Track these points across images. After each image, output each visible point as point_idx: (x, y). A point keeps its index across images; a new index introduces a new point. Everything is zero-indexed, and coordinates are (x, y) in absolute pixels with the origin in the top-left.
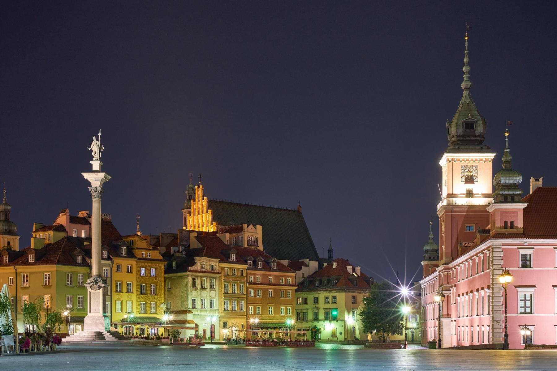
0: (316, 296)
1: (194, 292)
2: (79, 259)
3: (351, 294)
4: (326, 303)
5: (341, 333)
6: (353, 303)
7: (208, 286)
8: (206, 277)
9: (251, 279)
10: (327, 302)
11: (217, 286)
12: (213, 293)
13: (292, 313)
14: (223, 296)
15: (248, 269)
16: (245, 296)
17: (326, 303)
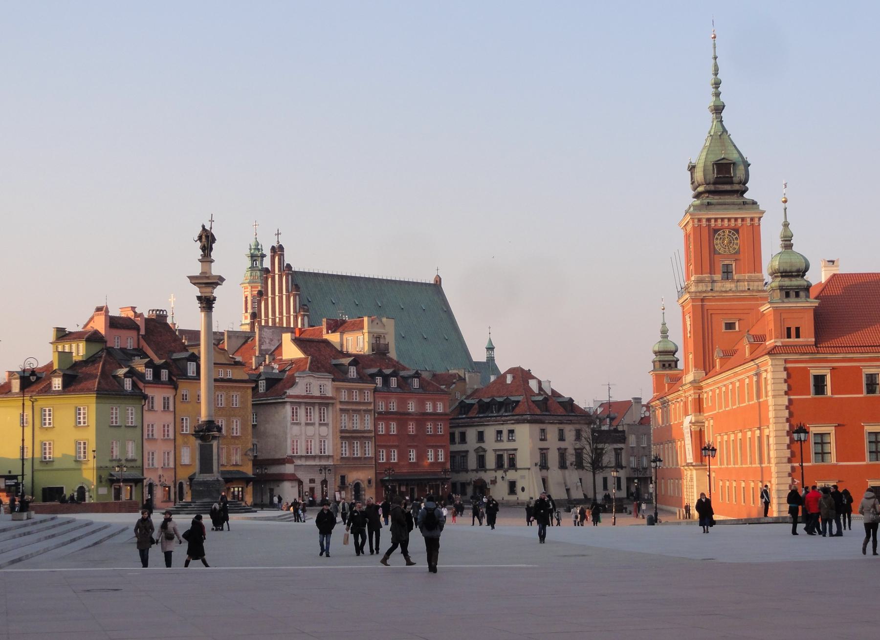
0: (481, 429)
1: (296, 429)
2: (128, 384)
3: (537, 427)
4: (497, 441)
5: (523, 489)
6: (541, 440)
7: (315, 416)
8: (313, 404)
9: (382, 407)
10: (498, 439)
11: (330, 419)
12: (324, 430)
13: (446, 458)
14: (339, 434)
15: (376, 390)
16: (373, 434)
17: (497, 441)
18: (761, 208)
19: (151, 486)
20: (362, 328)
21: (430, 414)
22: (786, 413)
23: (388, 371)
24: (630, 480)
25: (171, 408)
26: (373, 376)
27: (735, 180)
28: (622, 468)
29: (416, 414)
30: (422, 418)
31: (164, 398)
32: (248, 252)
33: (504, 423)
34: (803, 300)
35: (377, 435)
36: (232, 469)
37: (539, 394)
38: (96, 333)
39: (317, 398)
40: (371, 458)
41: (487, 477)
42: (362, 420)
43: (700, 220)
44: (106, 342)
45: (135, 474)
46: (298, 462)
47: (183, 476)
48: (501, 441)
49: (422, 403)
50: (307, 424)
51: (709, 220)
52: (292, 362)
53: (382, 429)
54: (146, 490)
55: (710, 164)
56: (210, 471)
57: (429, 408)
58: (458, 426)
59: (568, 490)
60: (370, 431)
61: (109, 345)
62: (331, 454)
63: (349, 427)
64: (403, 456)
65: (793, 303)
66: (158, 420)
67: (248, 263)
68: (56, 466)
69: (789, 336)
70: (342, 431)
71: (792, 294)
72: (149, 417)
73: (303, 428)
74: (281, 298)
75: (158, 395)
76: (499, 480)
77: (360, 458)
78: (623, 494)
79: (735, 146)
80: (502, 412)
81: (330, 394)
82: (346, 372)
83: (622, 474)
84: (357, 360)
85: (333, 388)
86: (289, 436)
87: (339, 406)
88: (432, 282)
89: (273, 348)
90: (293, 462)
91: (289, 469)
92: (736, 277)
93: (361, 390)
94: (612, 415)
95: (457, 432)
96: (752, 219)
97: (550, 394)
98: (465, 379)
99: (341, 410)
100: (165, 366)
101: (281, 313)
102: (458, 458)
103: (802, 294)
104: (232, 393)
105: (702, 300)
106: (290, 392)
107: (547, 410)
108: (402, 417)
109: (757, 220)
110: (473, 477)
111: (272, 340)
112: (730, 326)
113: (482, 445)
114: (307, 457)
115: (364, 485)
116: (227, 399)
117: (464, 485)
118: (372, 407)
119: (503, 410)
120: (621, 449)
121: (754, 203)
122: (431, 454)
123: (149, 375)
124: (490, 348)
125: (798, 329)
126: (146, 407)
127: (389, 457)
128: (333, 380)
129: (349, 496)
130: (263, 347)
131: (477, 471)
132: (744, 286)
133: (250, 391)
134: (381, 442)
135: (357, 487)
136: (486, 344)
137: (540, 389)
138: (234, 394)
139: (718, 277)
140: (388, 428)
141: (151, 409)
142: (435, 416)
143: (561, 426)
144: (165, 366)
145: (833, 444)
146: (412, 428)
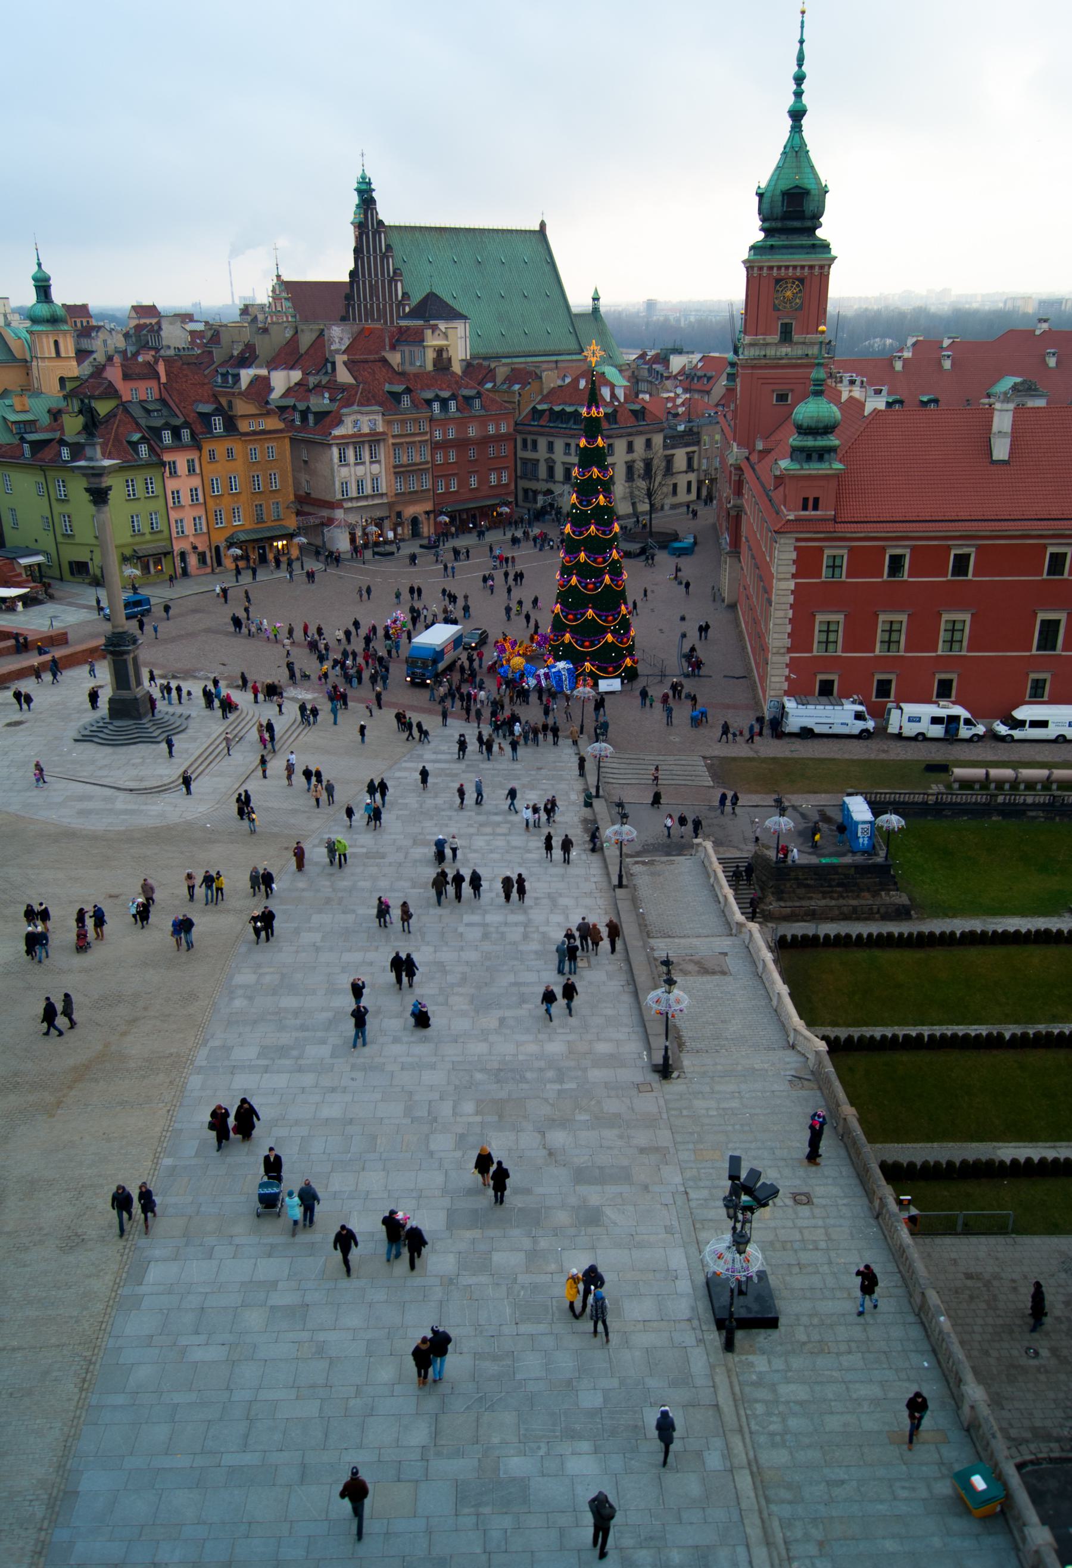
0: (551, 439)
1: (344, 471)
2: (143, 449)
4: (565, 454)
9: (438, 435)
12: (375, 468)
13: (510, 478)
14: (392, 470)
15: (431, 420)
16: (430, 465)
17: (565, 454)
18: (833, 253)
19: (183, 555)
20: (423, 341)
21: (492, 436)
22: (791, 599)
23: (445, 394)
24: (700, 483)
25: (198, 471)
26: (429, 402)
27: (808, 213)
28: (693, 471)
30: (485, 441)
31: (188, 461)
32: (356, 186)
33: (572, 436)
34: (825, 465)
35: (434, 466)
36: (273, 524)
37: (607, 405)
38: (111, 384)
39: (366, 435)
40: (428, 490)
41: (558, 489)
43: (761, 268)
44: (121, 397)
45: (161, 545)
46: (349, 505)
47: (219, 539)
48: (569, 454)
49: (484, 425)
50: (356, 464)
51: (771, 268)
52: (344, 388)
53: (439, 458)
54: (178, 560)
55: (778, 192)
56: (129, 689)
57: (491, 430)
58: (530, 433)
59: (634, 504)
60: (427, 463)
61: (124, 399)
63: (404, 460)
64: (463, 483)
65: (815, 468)
66: (183, 484)
67: (355, 199)
68: (77, 540)
69: (805, 508)
70: (395, 467)
71: (815, 456)
72: (171, 484)
73: (352, 469)
74: (375, 258)
75: (181, 461)
76: (566, 493)
77: (416, 492)
78: (693, 496)
79: (812, 167)
80: (571, 424)
81: (381, 430)
82: (399, 402)
83: (692, 477)
84: (412, 382)
85: (384, 421)
86: (337, 479)
87: (391, 441)
88: (537, 228)
89: (343, 348)
90: (342, 507)
91: (339, 514)
92: (796, 337)
93: (416, 421)
94: (709, 374)
95: (529, 438)
96: (822, 267)
97: (622, 400)
98: (541, 378)
99: (393, 444)
100: (187, 424)
101: (376, 275)
102: (529, 465)
103: (826, 456)
104: (266, 445)
105: (754, 367)
106: (337, 432)
107: (616, 423)
108: (461, 444)
109: (826, 269)
110: (542, 486)
111: (341, 339)
112: (782, 397)
113: (553, 456)
114: (358, 499)
115: (422, 518)
117: (536, 493)
119: (572, 422)
120: (694, 452)
121: (825, 247)
122: (493, 478)
123: (167, 436)
124: (596, 299)
125: (816, 501)
126: (167, 474)
127: (448, 487)
129: (406, 531)
130: (333, 348)
131: (547, 481)
132: (799, 351)
133: (287, 441)
135: (415, 521)
136: (591, 294)
137: (613, 395)
138: (270, 445)
139: (775, 338)
140: (446, 457)
141: (174, 474)
142: (499, 438)
143: (630, 439)
144: (187, 424)
145: (841, 633)
146: (472, 454)
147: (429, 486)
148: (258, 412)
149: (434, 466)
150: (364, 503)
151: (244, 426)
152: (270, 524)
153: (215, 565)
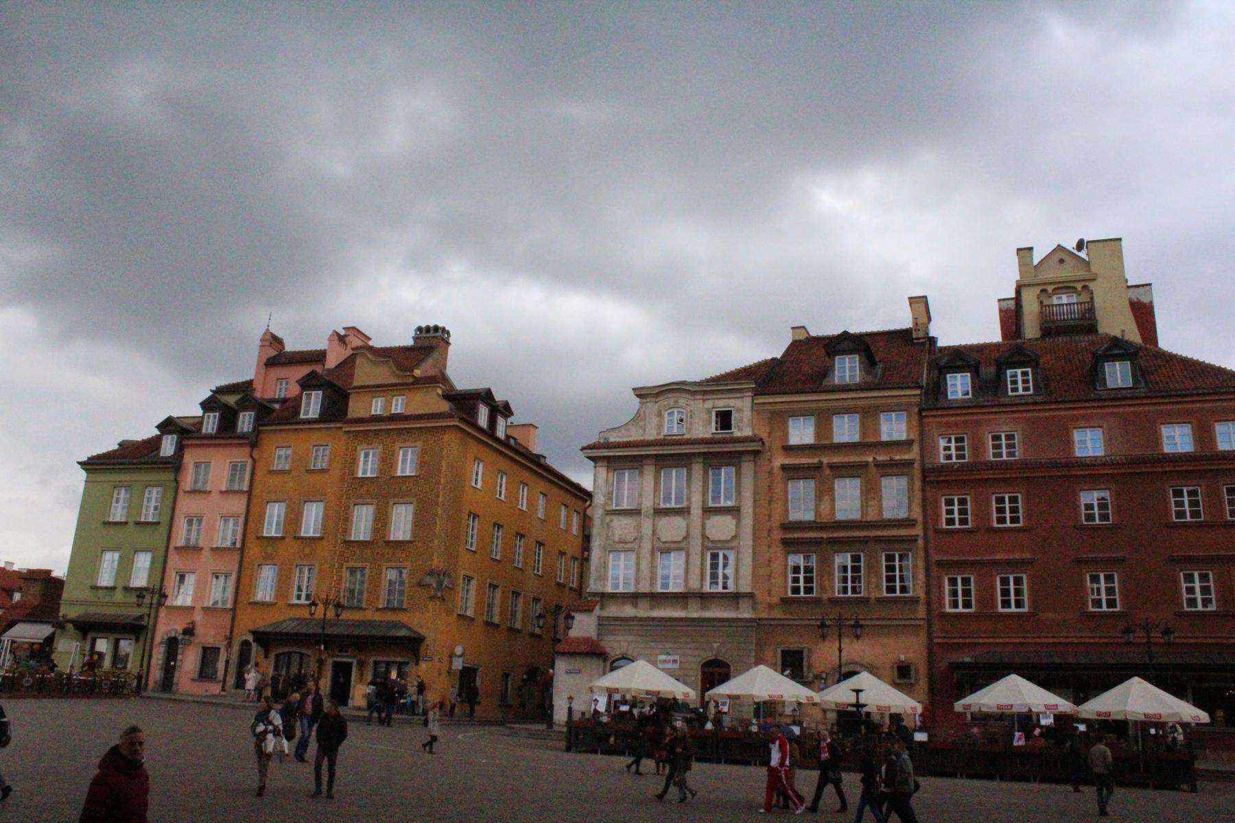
11: (748, 495)
12: (721, 527)
14: (778, 535)
16: (918, 531)
29: (1112, 464)
31: (234, 468)
36: (378, 617)
40: (914, 601)
42: (871, 492)
60: (908, 523)
62: (745, 588)
70: (788, 527)
81: (747, 432)
87: (779, 460)
99: (784, 468)
116: (383, 460)
118: (913, 454)
128: (757, 394)
134: (951, 554)
147: (916, 589)
148: (394, 380)
149: (934, 531)
150: (680, 614)
151: (356, 408)
152: (369, 615)
153: (231, 681)
